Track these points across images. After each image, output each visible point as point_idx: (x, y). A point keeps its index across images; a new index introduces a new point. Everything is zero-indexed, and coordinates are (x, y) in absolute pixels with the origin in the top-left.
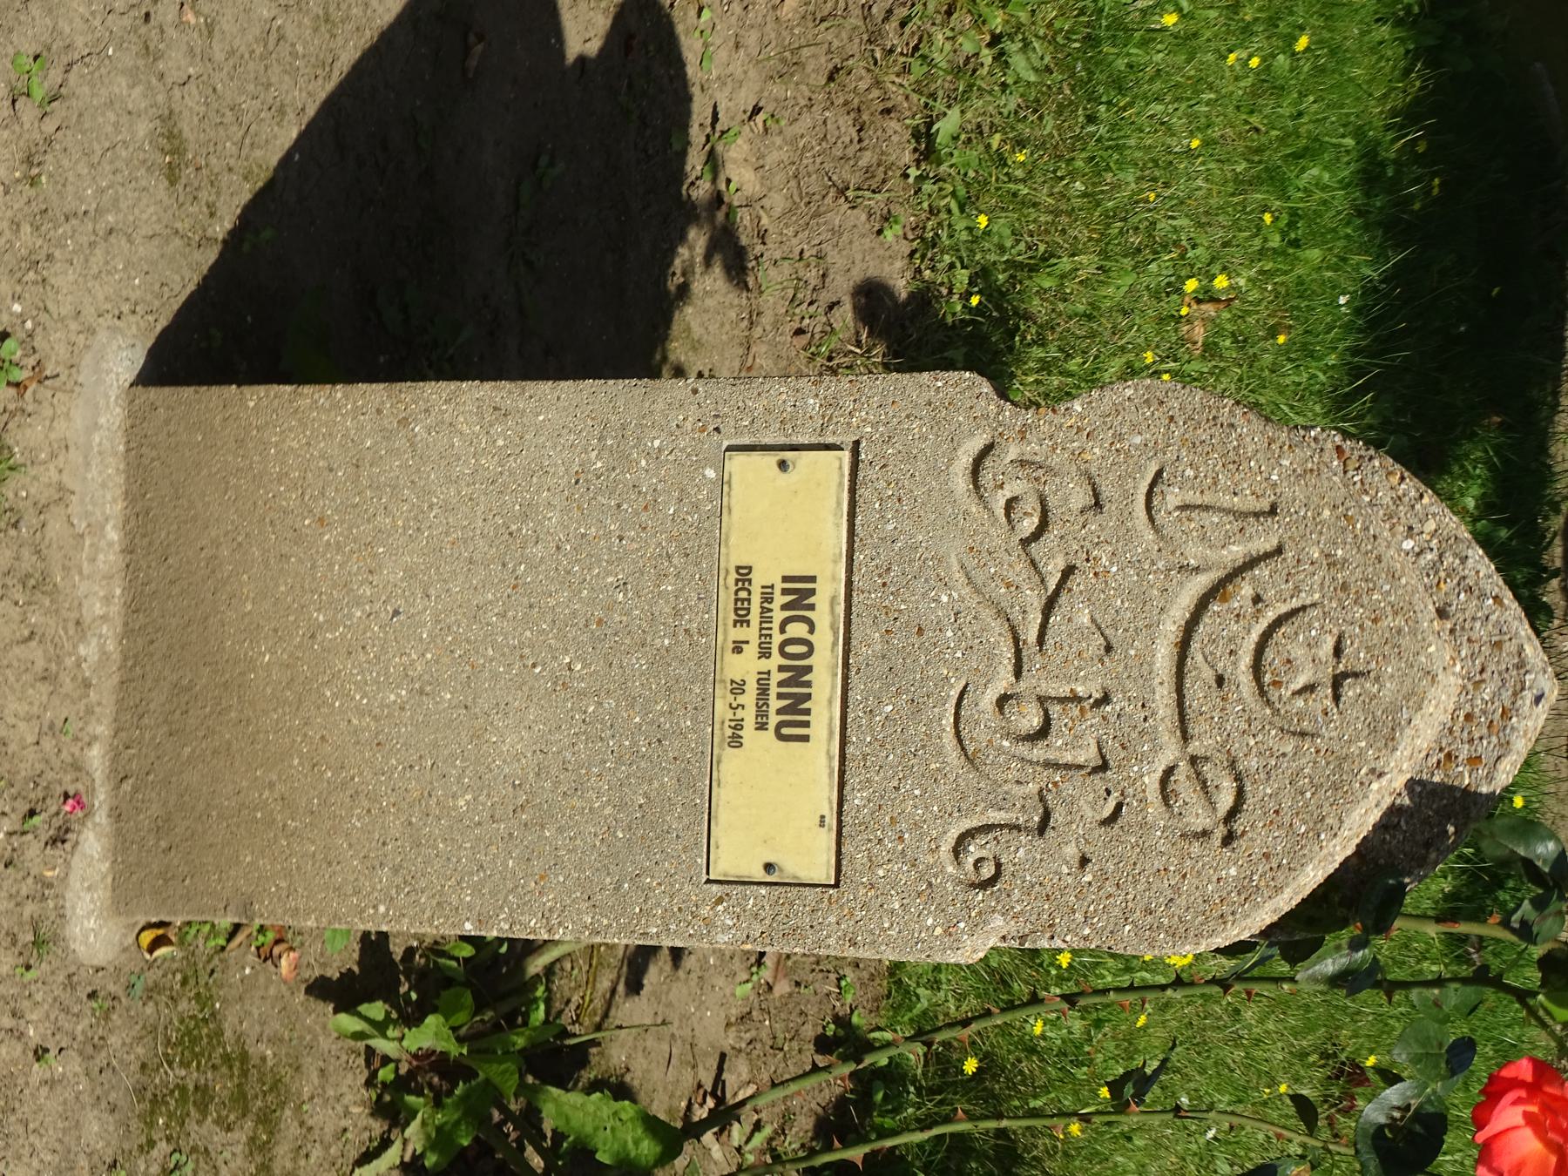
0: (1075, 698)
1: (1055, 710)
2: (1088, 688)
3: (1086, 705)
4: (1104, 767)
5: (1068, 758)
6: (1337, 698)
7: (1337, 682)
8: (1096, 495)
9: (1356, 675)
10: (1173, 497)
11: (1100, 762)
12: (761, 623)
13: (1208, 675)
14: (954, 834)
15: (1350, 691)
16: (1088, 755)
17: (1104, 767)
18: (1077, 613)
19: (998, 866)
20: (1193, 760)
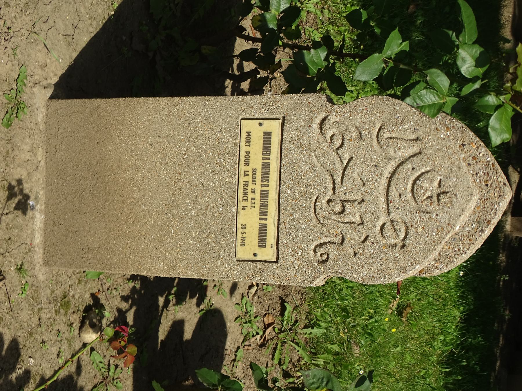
0: (354, 201)
1: (347, 206)
2: (357, 197)
3: (357, 202)
4: (362, 223)
5: (351, 219)
6: (439, 200)
7: (438, 195)
8: (361, 136)
9: (444, 193)
10: (385, 135)
11: (360, 221)
12: (253, 175)
13: (397, 194)
14: (313, 247)
15: (442, 197)
16: (357, 219)
17: (362, 223)
18: (353, 174)
19: (328, 258)
20: (392, 221)
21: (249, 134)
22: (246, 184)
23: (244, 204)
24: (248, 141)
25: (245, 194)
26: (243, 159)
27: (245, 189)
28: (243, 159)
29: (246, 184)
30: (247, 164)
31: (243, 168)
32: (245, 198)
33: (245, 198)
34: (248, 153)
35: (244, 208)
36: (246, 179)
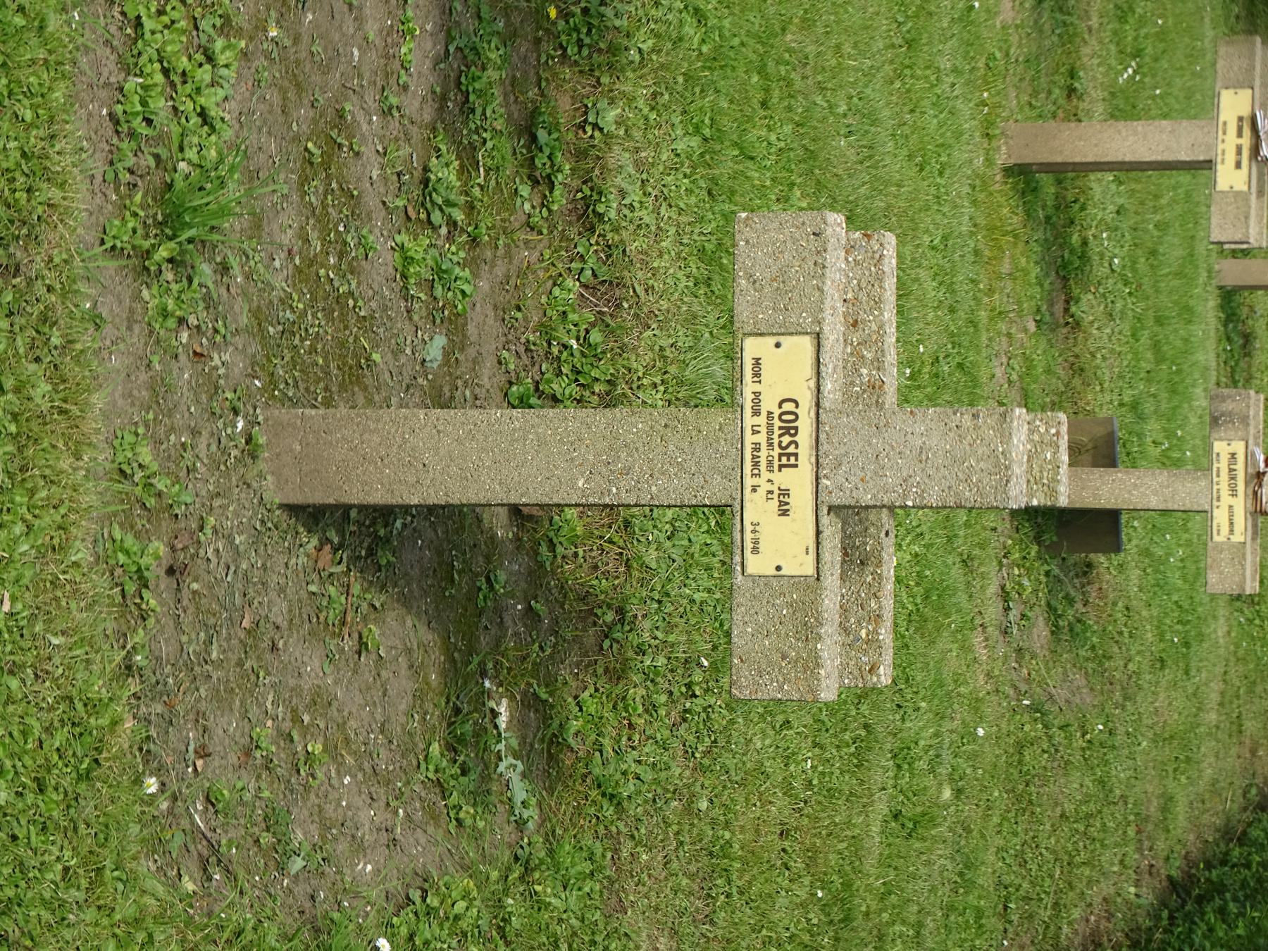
21: (757, 361)
22: (757, 447)
23: (755, 481)
24: (757, 374)
25: (756, 465)
26: (748, 405)
27: (754, 457)
28: (748, 405)
29: (757, 447)
30: (756, 413)
31: (749, 420)
32: (756, 472)
33: (756, 472)
34: (757, 394)
35: (754, 490)
36: (756, 438)
